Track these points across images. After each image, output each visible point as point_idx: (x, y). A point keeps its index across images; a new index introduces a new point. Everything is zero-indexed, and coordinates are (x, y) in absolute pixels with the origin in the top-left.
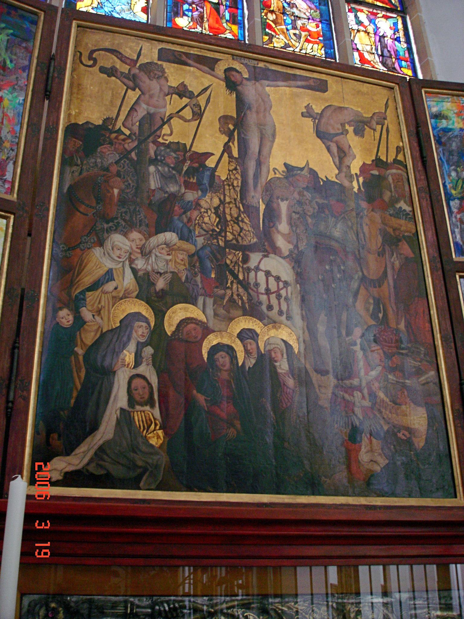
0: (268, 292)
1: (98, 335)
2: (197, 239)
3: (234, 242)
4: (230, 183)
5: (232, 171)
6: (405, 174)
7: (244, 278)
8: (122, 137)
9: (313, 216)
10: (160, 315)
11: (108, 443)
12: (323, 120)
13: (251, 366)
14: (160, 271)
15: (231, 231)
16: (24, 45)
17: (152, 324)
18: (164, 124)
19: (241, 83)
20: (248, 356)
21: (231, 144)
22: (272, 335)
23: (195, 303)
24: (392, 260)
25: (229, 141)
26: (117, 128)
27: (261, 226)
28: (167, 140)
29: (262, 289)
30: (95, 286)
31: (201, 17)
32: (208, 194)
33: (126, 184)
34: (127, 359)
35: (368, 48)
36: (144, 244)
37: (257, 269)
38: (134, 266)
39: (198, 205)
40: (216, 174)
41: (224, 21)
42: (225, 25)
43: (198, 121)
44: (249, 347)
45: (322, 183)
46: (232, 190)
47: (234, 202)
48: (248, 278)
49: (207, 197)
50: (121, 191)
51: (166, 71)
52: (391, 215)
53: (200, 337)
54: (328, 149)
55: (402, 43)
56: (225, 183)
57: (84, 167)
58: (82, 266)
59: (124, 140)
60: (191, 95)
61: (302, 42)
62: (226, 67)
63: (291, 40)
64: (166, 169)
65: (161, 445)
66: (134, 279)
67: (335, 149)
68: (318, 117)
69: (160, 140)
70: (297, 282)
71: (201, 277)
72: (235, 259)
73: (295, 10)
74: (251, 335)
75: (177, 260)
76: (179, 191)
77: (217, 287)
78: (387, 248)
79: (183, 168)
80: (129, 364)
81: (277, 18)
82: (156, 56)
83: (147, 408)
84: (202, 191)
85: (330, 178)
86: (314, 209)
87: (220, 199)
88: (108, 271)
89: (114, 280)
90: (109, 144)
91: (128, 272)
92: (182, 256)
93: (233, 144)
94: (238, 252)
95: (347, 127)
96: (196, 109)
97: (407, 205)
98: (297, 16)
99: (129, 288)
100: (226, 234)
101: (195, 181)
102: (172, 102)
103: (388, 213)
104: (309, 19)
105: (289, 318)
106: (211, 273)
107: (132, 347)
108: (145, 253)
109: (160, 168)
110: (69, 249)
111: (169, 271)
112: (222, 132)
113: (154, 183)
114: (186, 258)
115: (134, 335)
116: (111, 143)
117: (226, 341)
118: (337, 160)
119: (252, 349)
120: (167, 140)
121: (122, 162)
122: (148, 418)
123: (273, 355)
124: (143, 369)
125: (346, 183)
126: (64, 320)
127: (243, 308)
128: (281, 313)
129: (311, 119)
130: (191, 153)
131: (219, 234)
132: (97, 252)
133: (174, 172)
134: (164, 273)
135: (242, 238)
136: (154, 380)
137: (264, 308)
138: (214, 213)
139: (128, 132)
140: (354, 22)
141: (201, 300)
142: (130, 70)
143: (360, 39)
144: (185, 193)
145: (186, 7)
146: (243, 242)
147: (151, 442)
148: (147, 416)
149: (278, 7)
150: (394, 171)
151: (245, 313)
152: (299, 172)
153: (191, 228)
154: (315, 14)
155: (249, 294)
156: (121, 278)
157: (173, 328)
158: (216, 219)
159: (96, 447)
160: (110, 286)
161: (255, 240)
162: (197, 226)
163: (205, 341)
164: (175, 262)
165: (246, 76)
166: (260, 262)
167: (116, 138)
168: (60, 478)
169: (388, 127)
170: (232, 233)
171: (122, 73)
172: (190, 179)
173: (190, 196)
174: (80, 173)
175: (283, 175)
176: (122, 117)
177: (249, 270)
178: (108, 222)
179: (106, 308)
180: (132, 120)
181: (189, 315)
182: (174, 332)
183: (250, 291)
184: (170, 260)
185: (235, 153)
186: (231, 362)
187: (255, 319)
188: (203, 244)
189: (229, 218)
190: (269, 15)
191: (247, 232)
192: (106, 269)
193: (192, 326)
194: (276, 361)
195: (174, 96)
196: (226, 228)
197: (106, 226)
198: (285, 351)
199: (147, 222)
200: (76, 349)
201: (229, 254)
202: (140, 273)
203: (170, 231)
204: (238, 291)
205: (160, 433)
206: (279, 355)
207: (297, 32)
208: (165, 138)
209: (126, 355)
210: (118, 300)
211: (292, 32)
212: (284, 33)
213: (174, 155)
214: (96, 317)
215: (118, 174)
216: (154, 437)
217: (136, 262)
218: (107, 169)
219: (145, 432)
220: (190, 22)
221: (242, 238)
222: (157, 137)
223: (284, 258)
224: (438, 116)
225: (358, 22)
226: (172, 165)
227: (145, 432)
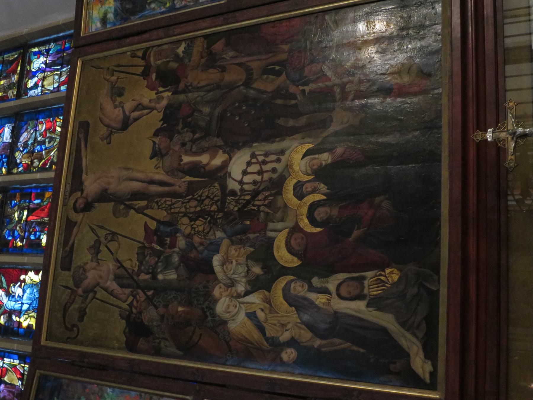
0: (260, 173)
1: (303, 326)
2: (217, 237)
3: (219, 203)
4: (169, 208)
5: (159, 206)
6: (154, 48)
7: (249, 194)
8: (135, 303)
9: (194, 133)
10: (284, 271)
11: (397, 319)
12: (114, 124)
13: (326, 187)
14: (246, 271)
15: (209, 206)
16: (65, 387)
17: (292, 277)
18: (122, 266)
19: (86, 198)
20: (318, 190)
21: (136, 207)
22: (298, 168)
23: (273, 240)
24: (228, 58)
25: (134, 209)
26: (127, 307)
27: (204, 179)
28: (136, 264)
29: (258, 178)
30: (261, 329)
32: (179, 228)
33: (173, 300)
34: (323, 301)
35: (56, 77)
36: (224, 284)
37: (241, 182)
38: (243, 294)
39: (189, 236)
40: (162, 220)
41: (42, 204)
42: (45, 203)
43: (119, 236)
44: (309, 189)
45: (165, 125)
46: (175, 206)
47: (185, 204)
48: (250, 191)
49: (181, 228)
50: (180, 304)
51: (79, 264)
52: (190, 61)
53: (301, 235)
54: (136, 119)
55: (50, 47)
56: (169, 212)
57: (161, 336)
58: (244, 340)
59: (137, 302)
60: (98, 242)
62: (73, 212)
64: (160, 264)
65: (399, 270)
66: (254, 294)
67: (136, 114)
68: (110, 129)
69: (136, 269)
70: (251, 146)
71: (250, 233)
72: (233, 203)
73: (30, 143)
74: (299, 188)
75: (236, 254)
76: (178, 253)
77: (258, 219)
78: (218, 64)
79: (158, 250)
80: (328, 300)
82: (67, 273)
83: (366, 283)
84: (176, 233)
85: (161, 117)
86: (187, 131)
87: (183, 217)
88: (248, 317)
89: (255, 311)
90: (141, 314)
91: (248, 299)
92: (233, 251)
93: (136, 205)
94: (227, 200)
95: (117, 103)
96: (109, 238)
97: (180, 46)
98: (34, 141)
99: (262, 299)
100: (212, 211)
101: (169, 239)
102: (104, 259)
103: (188, 63)
105: (283, 152)
106: (246, 225)
107: (313, 296)
108: (232, 283)
109: (159, 270)
110: (230, 351)
111: (246, 263)
112: (126, 215)
113: (172, 276)
114: (234, 247)
115: (302, 294)
116: (140, 313)
117: (305, 210)
118: (145, 112)
119: (311, 187)
120: (136, 264)
121: (155, 303)
122: (375, 282)
123: (315, 167)
124: (332, 287)
125: (164, 102)
126: (292, 356)
127: (275, 195)
128: (278, 161)
129: (112, 136)
130: (145, 242)
131: (212, 217)
132: (232, 326)
133: (162, 258)
134: (248, 267)
135: (215, 196)
136: (342, 276)
137: (275, 176)
138: (195, 221)
139: (131, 298)
140: (36, 91)
141: (270, 234)
142: (80, 296)
143: (50, 85)
144: (179, 248)
145: (32, 237)
146: (218, 196)
147: (396, 280)
148: (373, 282)
149: (28, 158)
150: (152, 59)
151: (280, 193)
152: (157, 146)
153: (208, 242)
154: (31, 126)
155: (263, 190)
156: (254, 305)
157: (296, 259)
158: (200, 220)
159: (402, 330)
160: (261, 315)
161: (216, 185)
162: (207, 237)
163: (305, 230)
164: (237, 256)
165: (79, 194)
166: (235, 180)
167: (136, 308)
168: (430, 363)
169: (115, 66)
170: (212, 205)
171: (83, 303)
172: (167, 243)
173: (181, 243)
174: (167, 340)
175: (160, 161)
176: (120, 303)
177: (242, 190)
178: (207, 317)
179: (279, 319)
180: (121, 294)
181: (283, 245)
182: (299, 258)
183: (261, 188)
184: (236, 261)
185: (143, 203)
186: (323, 205)
187: (285, 184)
188: (221, 232)
189: (198, 209)
190: (35, 165)
191: (210, 192)
192: (246, 318)
193: (293, 242)
194: (321, 164)
195: (99, 257)
196: (207, 211)
197: (209, 318)
198: (312, 156)
199: (205, 282)
200: (316, 347)
201: (229, 208)
202: (249, 288)
203: (212, 261)
204: (260, 200)
205: (388, 271)
206: (315, 162)
208: (134, 265)
209: (320, 302)
210: (272, 308)
211: (47, 145)
213: (148, 258)
214: (287, 328)
215: (166, 306)
216: (392, 277)
217: (239, 291)
218: (162, 316)
219: (387, 285)
221: (215, 196)
222: (134, 273)
223: (231, 159)
224: (104, 21)
225: (35, 87)
226: (157, 259)
227: (387, 285)
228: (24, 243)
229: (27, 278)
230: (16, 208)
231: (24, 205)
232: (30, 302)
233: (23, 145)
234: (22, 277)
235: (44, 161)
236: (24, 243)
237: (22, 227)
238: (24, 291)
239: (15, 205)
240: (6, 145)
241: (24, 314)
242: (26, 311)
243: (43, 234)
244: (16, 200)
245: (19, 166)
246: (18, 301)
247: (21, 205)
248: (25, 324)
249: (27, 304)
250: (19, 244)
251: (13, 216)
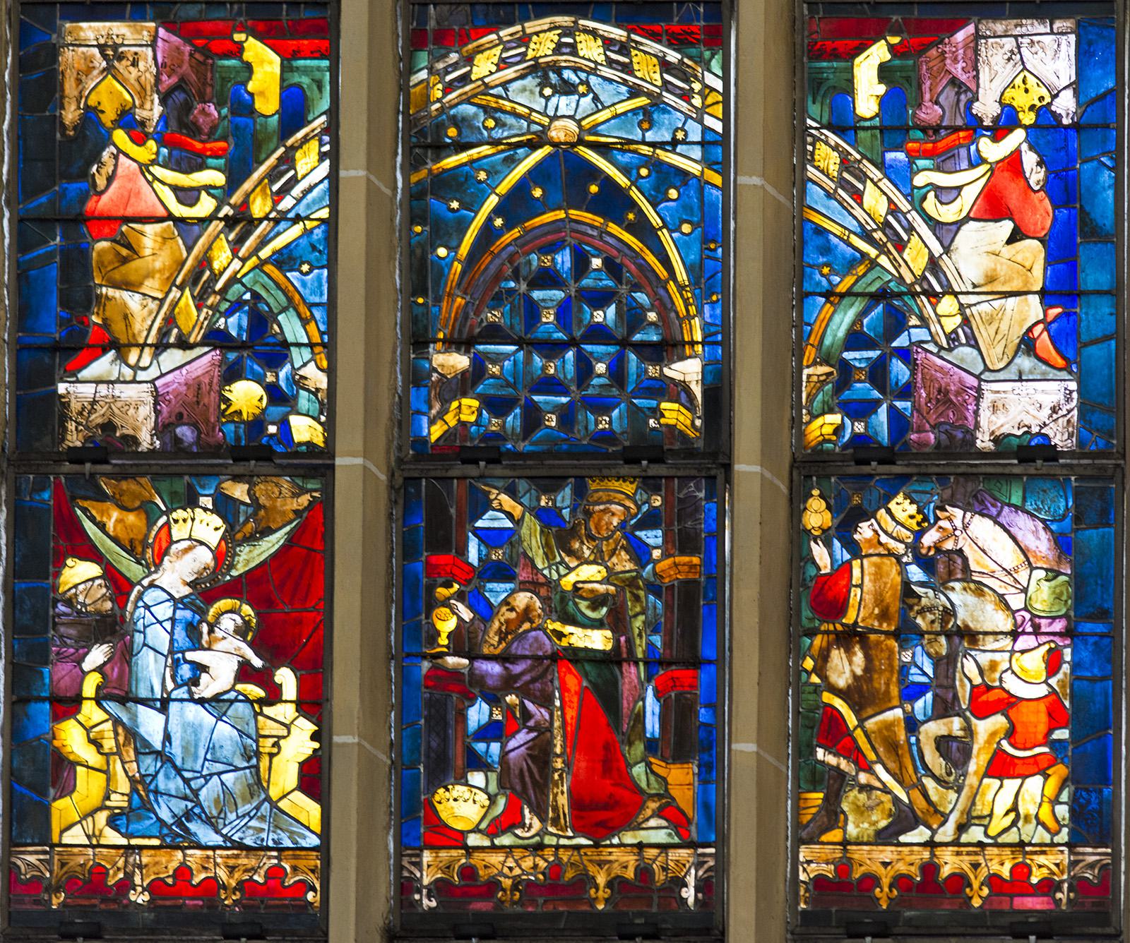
31: (540, 753)
41: (639, 748)
42: (639, 771)
61: (972, 780)
63: (929, 783)
81: (868, 669)
104: (1015, 634)
145: (478, 714)
149: (879, 600)
190: (837, 656)
207: (956, 725)
211: (933, 729)
212: (893, 747)
220: (492, 799)
228: (451, 661)
229: (284, 711)
230: (623, 563)
231: (638, 623)
232: (176, 750)
233: (949, 545)
234: (286, 678)
235: (851, 720)
236: (451, 661)
237: (526, 626)
238: (217, 703)
239: (640, 553)
240: (959, 409)
241: (117, 722)
242: (133, 735)
243: (493, 788)
244: (666, 555)
245: (837, 544)
246: (176, 664)
247: (637, 598)
248: (71, 737)
249: (167, 737)
250: (446, 625)
251: (587, 553)
